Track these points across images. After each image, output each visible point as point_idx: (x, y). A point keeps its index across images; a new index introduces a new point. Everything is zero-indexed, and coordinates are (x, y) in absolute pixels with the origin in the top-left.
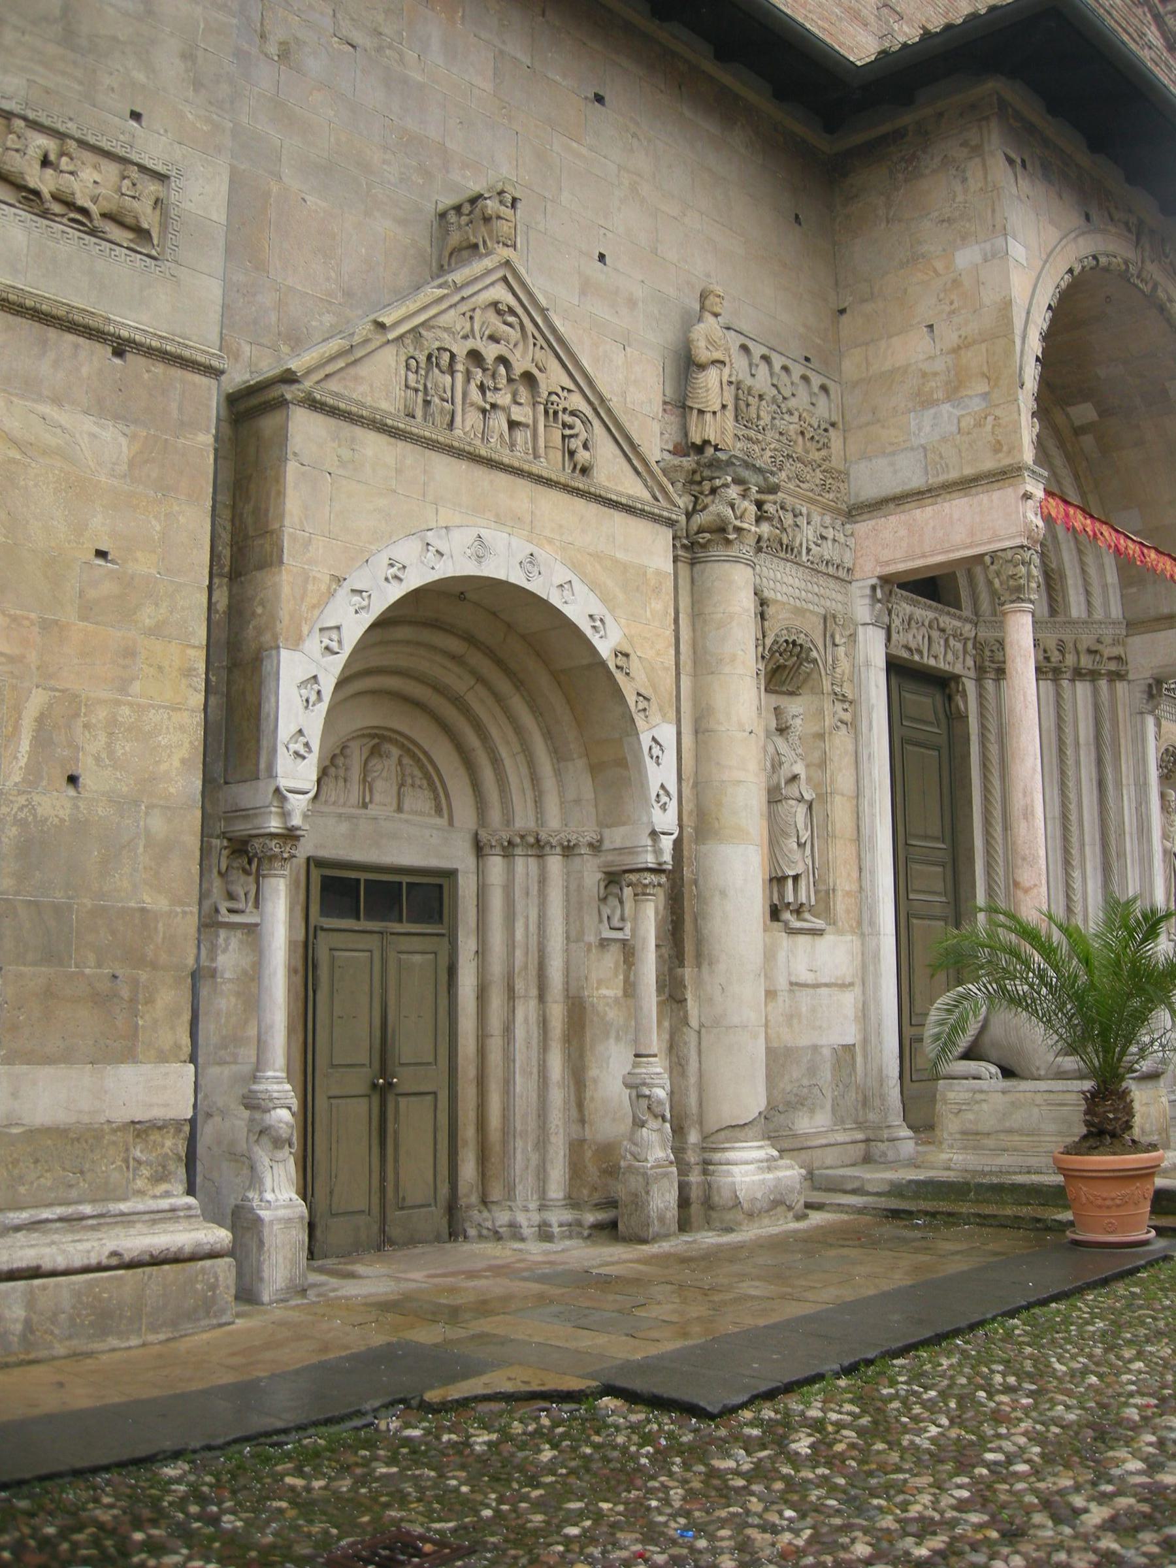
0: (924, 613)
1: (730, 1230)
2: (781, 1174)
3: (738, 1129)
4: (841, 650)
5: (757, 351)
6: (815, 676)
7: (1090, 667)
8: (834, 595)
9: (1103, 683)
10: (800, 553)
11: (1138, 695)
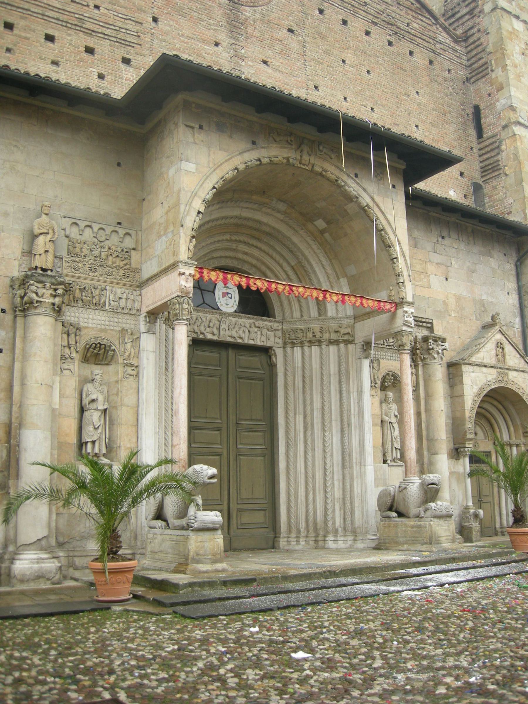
0: (245, 321)
1: (13, 587)
2: (43, 565)
3: (28, 546)
4: (129, 346)
5: (82, 224)
6: (115, 356)
7: (335, 339)
8: (128, 321)
9: (342, 346)
10: (105, 306)
11: (359, 350)
